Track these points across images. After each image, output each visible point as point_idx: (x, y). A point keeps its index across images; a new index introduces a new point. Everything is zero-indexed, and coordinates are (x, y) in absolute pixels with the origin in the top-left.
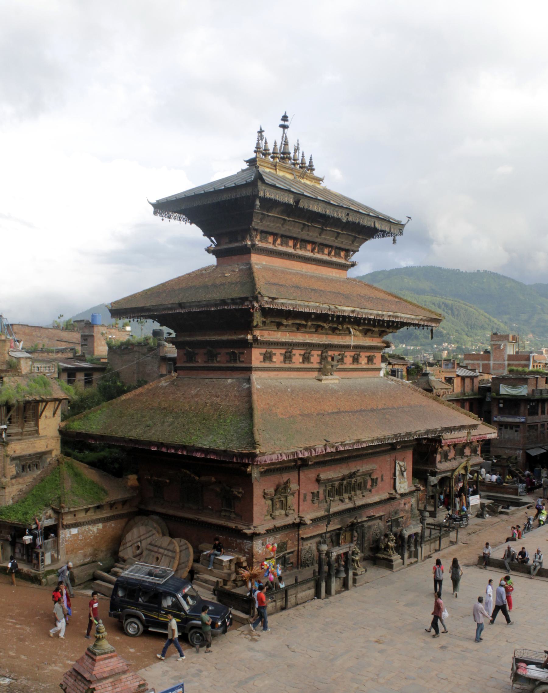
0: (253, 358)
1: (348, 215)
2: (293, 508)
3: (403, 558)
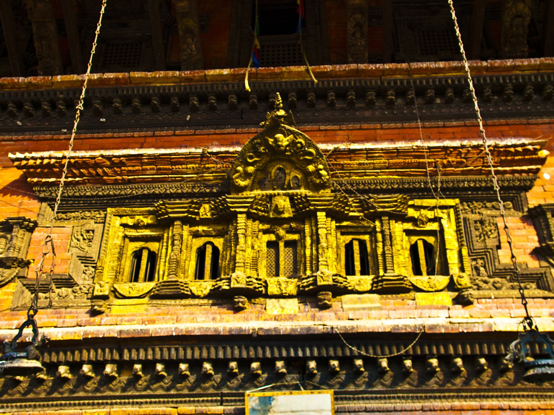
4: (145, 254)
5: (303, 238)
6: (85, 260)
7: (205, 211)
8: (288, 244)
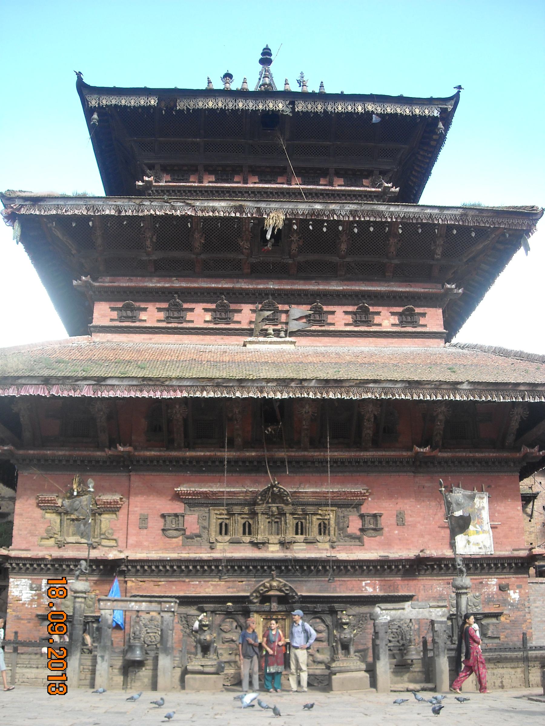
0: (95, 315)
1: (292, 103)
2: (114, 537)
3: (371, 670)
4: (224, 524)
5: (281, 521)
6: (204, 528)
7: (246, 509)
8: (275, 522)
